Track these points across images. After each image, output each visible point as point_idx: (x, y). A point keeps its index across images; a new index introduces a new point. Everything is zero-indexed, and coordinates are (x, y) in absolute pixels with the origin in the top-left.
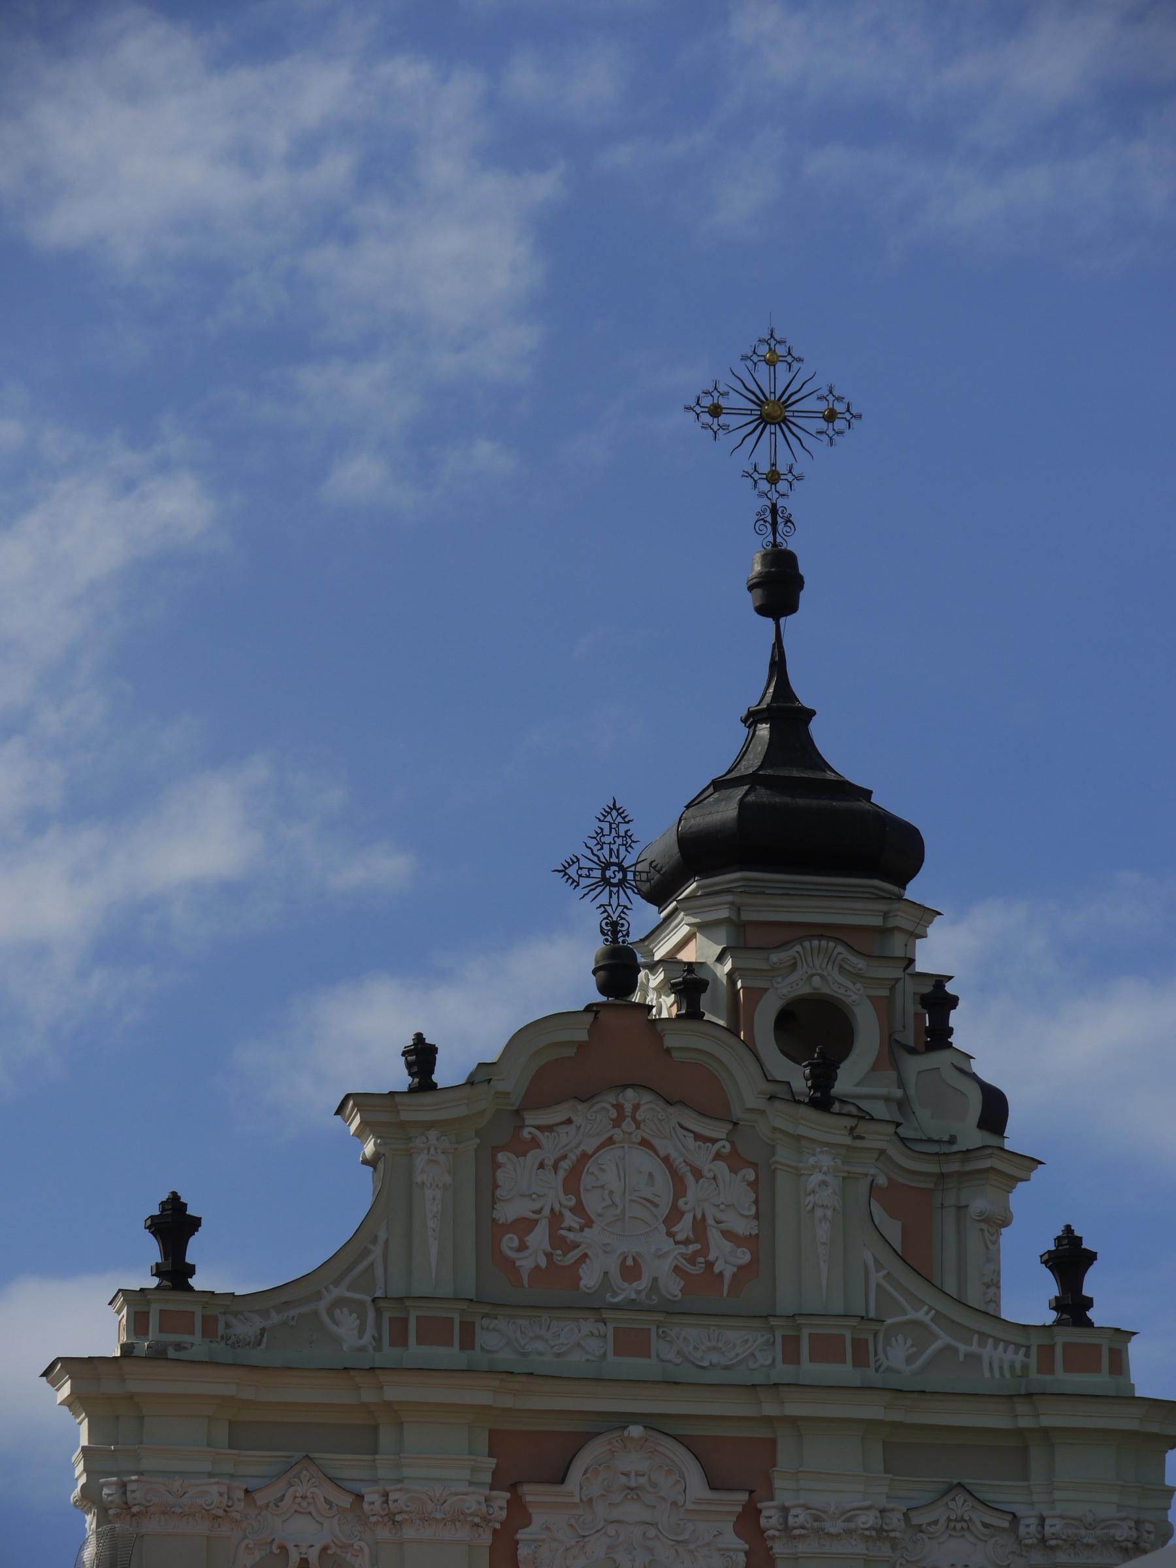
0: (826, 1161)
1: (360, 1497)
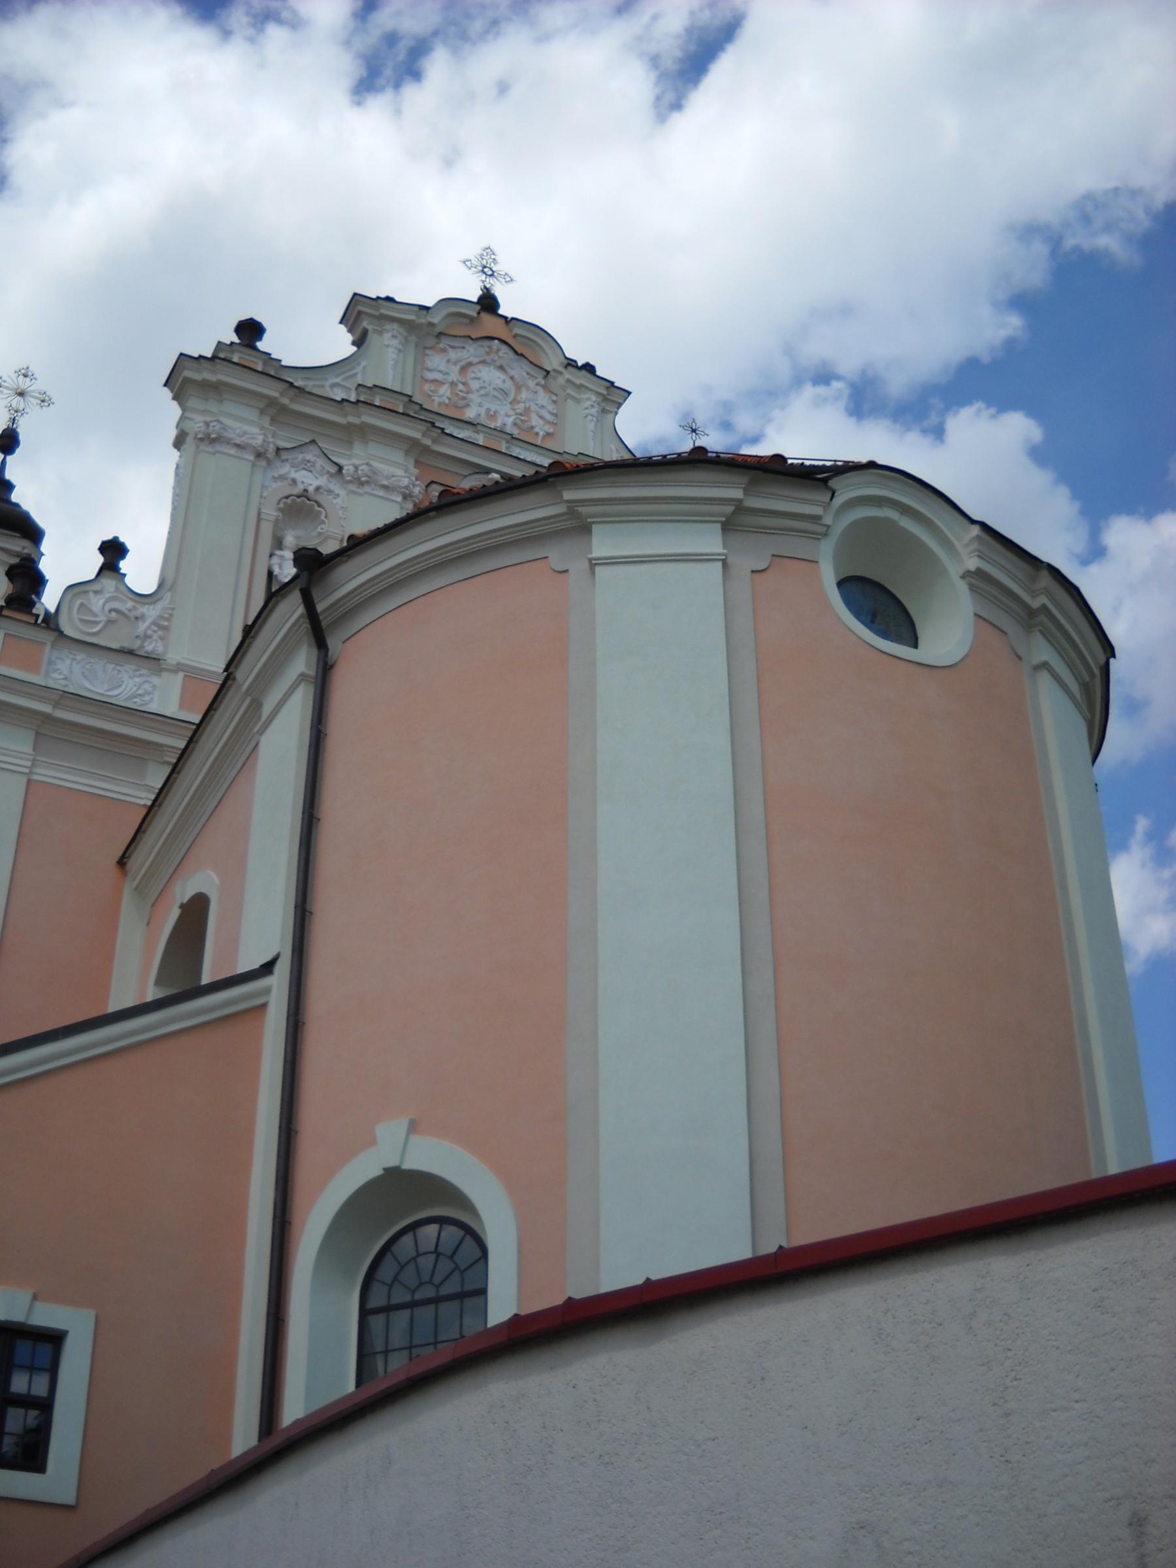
0: (593, 398)
1: (340, 468)
